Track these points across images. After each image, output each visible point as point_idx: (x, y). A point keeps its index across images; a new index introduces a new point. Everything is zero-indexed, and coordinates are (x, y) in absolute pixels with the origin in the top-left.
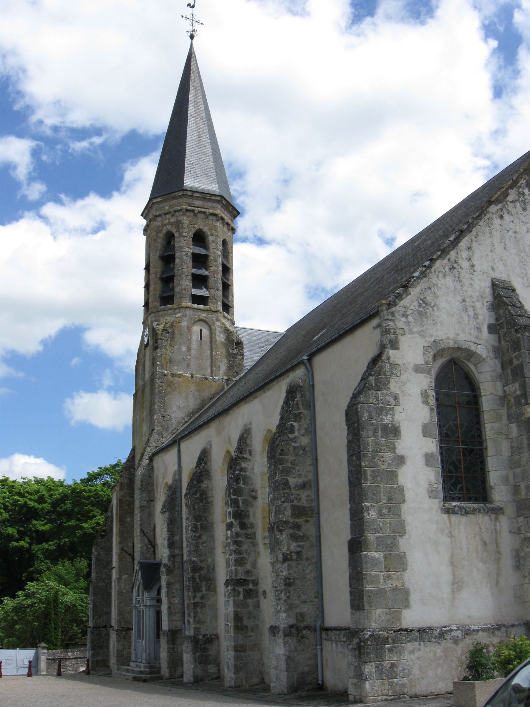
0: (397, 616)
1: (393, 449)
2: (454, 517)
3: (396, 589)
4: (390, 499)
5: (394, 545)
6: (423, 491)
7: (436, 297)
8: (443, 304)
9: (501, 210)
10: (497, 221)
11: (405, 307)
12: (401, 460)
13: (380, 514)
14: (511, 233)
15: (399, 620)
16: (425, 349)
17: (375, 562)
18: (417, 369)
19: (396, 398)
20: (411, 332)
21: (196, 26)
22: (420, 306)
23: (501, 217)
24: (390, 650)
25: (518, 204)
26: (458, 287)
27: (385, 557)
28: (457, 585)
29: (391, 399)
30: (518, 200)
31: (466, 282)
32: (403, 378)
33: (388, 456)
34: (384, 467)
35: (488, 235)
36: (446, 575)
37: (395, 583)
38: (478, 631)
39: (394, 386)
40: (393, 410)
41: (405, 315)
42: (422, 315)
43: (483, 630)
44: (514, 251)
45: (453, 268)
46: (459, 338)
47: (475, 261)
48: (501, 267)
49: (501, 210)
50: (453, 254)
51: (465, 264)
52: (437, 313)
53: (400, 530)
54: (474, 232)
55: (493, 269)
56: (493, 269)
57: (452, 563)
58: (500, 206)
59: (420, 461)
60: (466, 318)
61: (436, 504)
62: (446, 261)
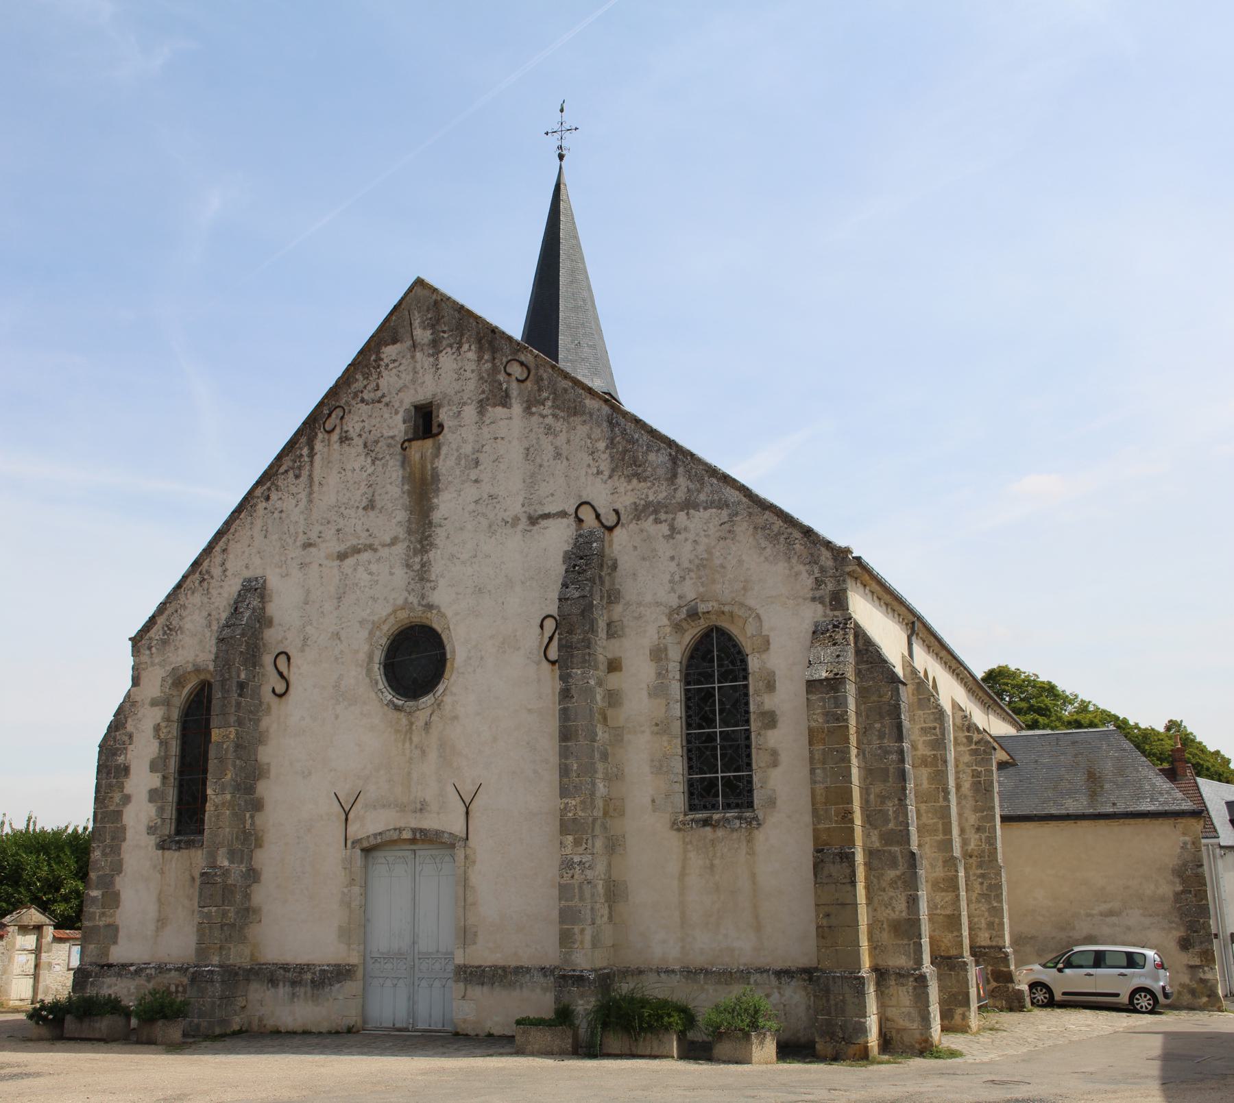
0: (105, 952)
1: (121, 787)
2: (167, 853)
3: (109, 926)
4: (113, 839)
5: (112, 883)
6: (143, 829)
7: (182, 618)
8: (188, 625)
9: (269, 489)
10: (261, 505)
11: (150, 639)
12: (127, 799)
13: (104, 854)
14: (276, 515)
15: (107, 955)
16: (163, 680)
17: (94, 899)
18: (154, 703)
19: (131, 736)
20: (153, 664)
21: (569, 140)
22: (165, 633)
23: (268, 498)
24: (92, 983)
25: (291, 474)
26: (206, 600)
27: (103, 895)
28: (162, 922)
29: (126, 738)
30: (292, 468)
31: (214, 592)
32: (140, 715)
33: (117, 797)
34: (112, 808)
35: (248, 526)
36: (152, 910)
37: (109, 920)
38: (170, 970)
39: (130, 727)
40: (126, 749)
41: (150, 648)
42: (165, 643)
43: (177, 969)
44: (275, 537)
45: (204, 580)
46: (198, 660)
47: (228, 565)
48: (257, 561)
49: (269, 489)
50: (206, 564)
51: (216, 571)
52: (180, 637)
53: (118, 868)
54: (232, 530)
55: (247, 567)
56: (247, 567)
57: (159, 900)
58: (268, 484)
59: (144, 796)
60: (208, 634)
61: (152, 841)
62: (197, 575)
